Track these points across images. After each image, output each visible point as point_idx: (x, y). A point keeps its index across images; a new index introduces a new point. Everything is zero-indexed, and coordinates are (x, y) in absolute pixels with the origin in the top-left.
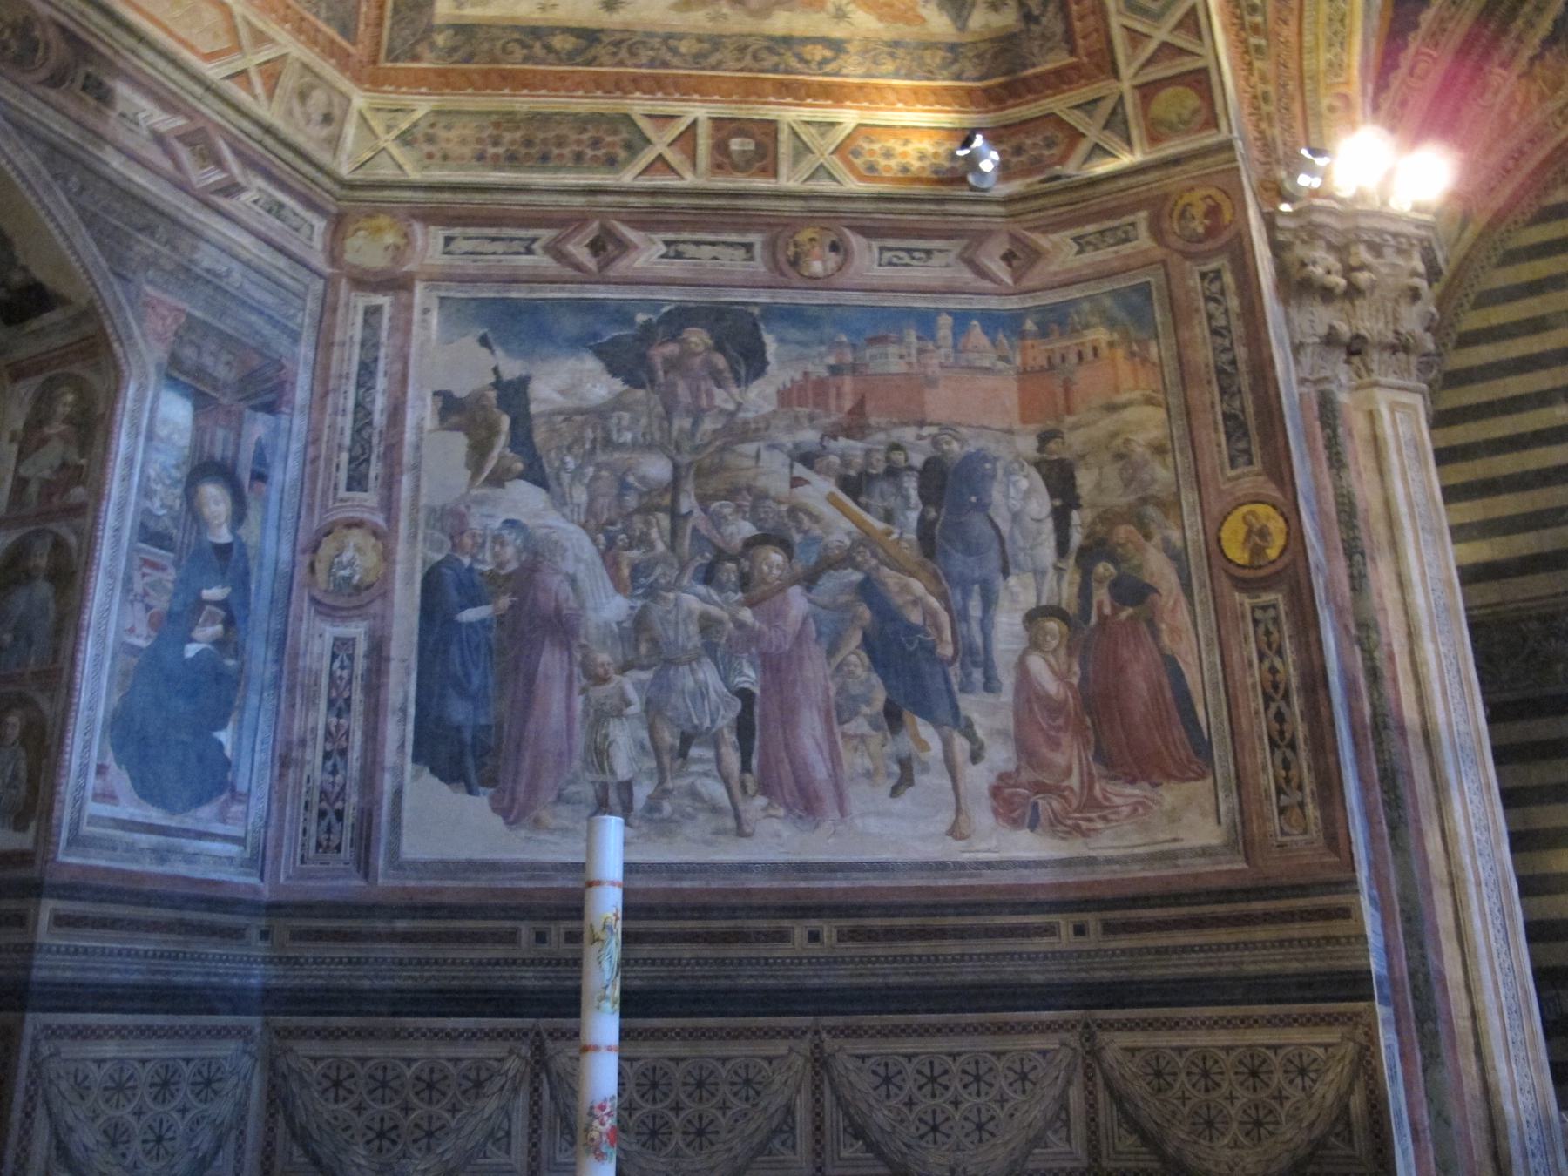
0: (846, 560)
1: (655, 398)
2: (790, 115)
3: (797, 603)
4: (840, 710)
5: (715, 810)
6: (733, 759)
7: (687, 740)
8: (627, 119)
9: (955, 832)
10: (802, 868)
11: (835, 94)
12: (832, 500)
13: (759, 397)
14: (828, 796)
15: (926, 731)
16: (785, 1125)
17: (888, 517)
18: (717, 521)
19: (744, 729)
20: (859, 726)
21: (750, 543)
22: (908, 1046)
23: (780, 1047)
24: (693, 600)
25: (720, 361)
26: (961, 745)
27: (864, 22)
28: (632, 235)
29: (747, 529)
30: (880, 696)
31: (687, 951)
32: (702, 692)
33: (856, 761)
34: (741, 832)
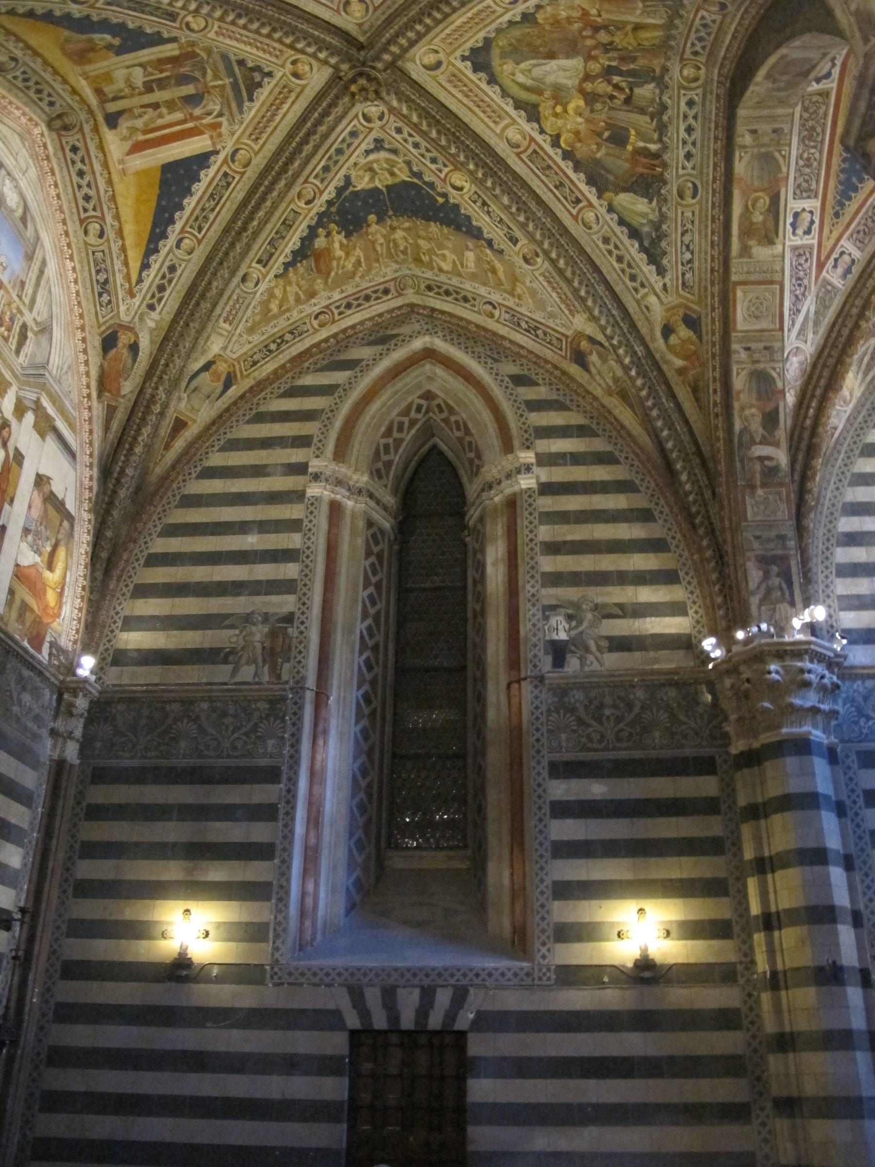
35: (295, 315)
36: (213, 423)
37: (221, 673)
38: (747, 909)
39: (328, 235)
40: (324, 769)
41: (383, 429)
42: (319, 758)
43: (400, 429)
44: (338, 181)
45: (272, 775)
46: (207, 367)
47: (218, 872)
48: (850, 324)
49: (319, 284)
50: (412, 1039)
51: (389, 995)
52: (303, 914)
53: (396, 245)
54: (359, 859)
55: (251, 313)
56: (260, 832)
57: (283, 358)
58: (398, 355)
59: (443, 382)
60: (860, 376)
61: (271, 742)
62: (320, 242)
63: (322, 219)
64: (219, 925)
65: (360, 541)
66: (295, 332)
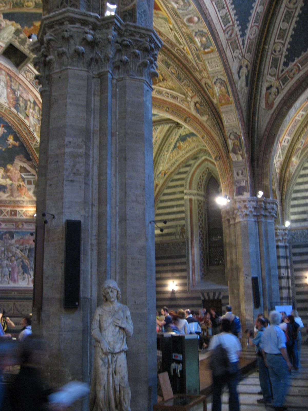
0: (20, 258)
1: (3, 242)
2: (18, 209)
3: (15, 262)
4: (18, 273)
5: (6, 282)
6: (8, 277)
7: (4, 275)
8: (1, 210)
9: (28, 284)
10: (14, 287)
11: (23, 207)
12: (20, 253)
13: (13, 241)
14: (17, 281)
15: (26, 275)
16: (11, 309)
17: (25, 254)
18: (8, 254)
19: (10, 274)
20: (20, 274)
21: (11, 257)
22: (22, 303)
23: (11, 303)
24: (6, 262)
25: (10, 238)
26: (29, 276)
27: (26, 199)
28: (2, 223)
29: (11, 255)
30: (22, 271)
31: (4, 294)
32: (6, 271)
33: (19, 277)
34: (9, 283)
35: (176, 158)
36: (163, 183)
37: (173, 237)
38: (291, 270)
39: (179, 143)
40: (194, 253)
41: (199, 179)
42: (193, 252)
43: (203, 176)
44: (178, 135)
45: (184, 256)
46: (160, 173)
47: (177, 275)
48: (290, 153)
49: (180, 151)
50: (213, 300)
51: (208, 294)
52: (193, 281)
53: (194, 140)
54: (203, 269)
55: (167, 159)
56: (184, 267)
57: (176, 165)
58: (199, 161)
59: (210, 166)
60: (298, 159)
61: (184, 250)
62: (178, 144)
63: (177, 141)
64: (179, 284)
65: (197, 206)
66: (177, 161)
